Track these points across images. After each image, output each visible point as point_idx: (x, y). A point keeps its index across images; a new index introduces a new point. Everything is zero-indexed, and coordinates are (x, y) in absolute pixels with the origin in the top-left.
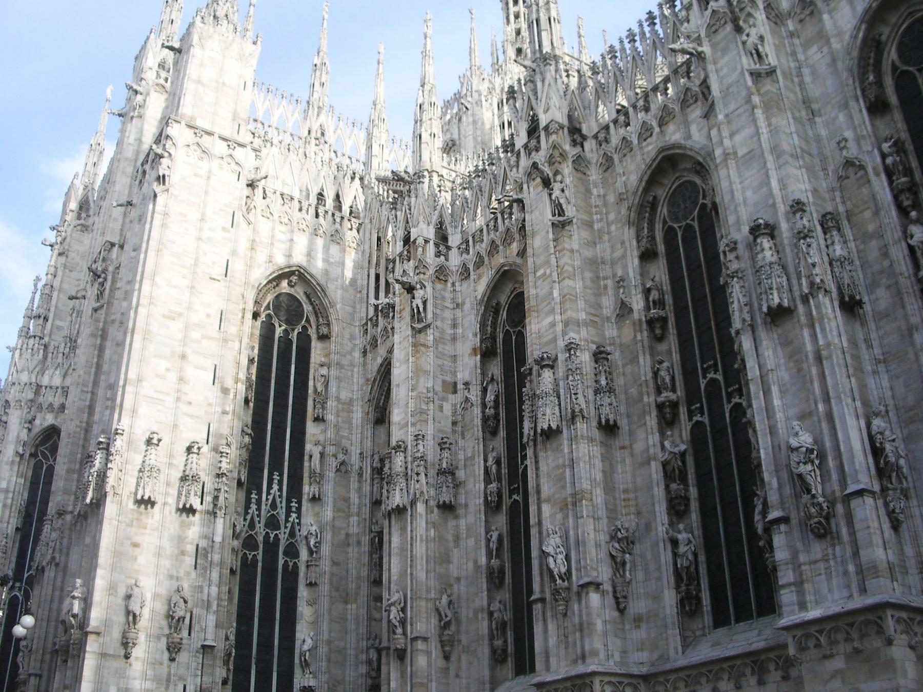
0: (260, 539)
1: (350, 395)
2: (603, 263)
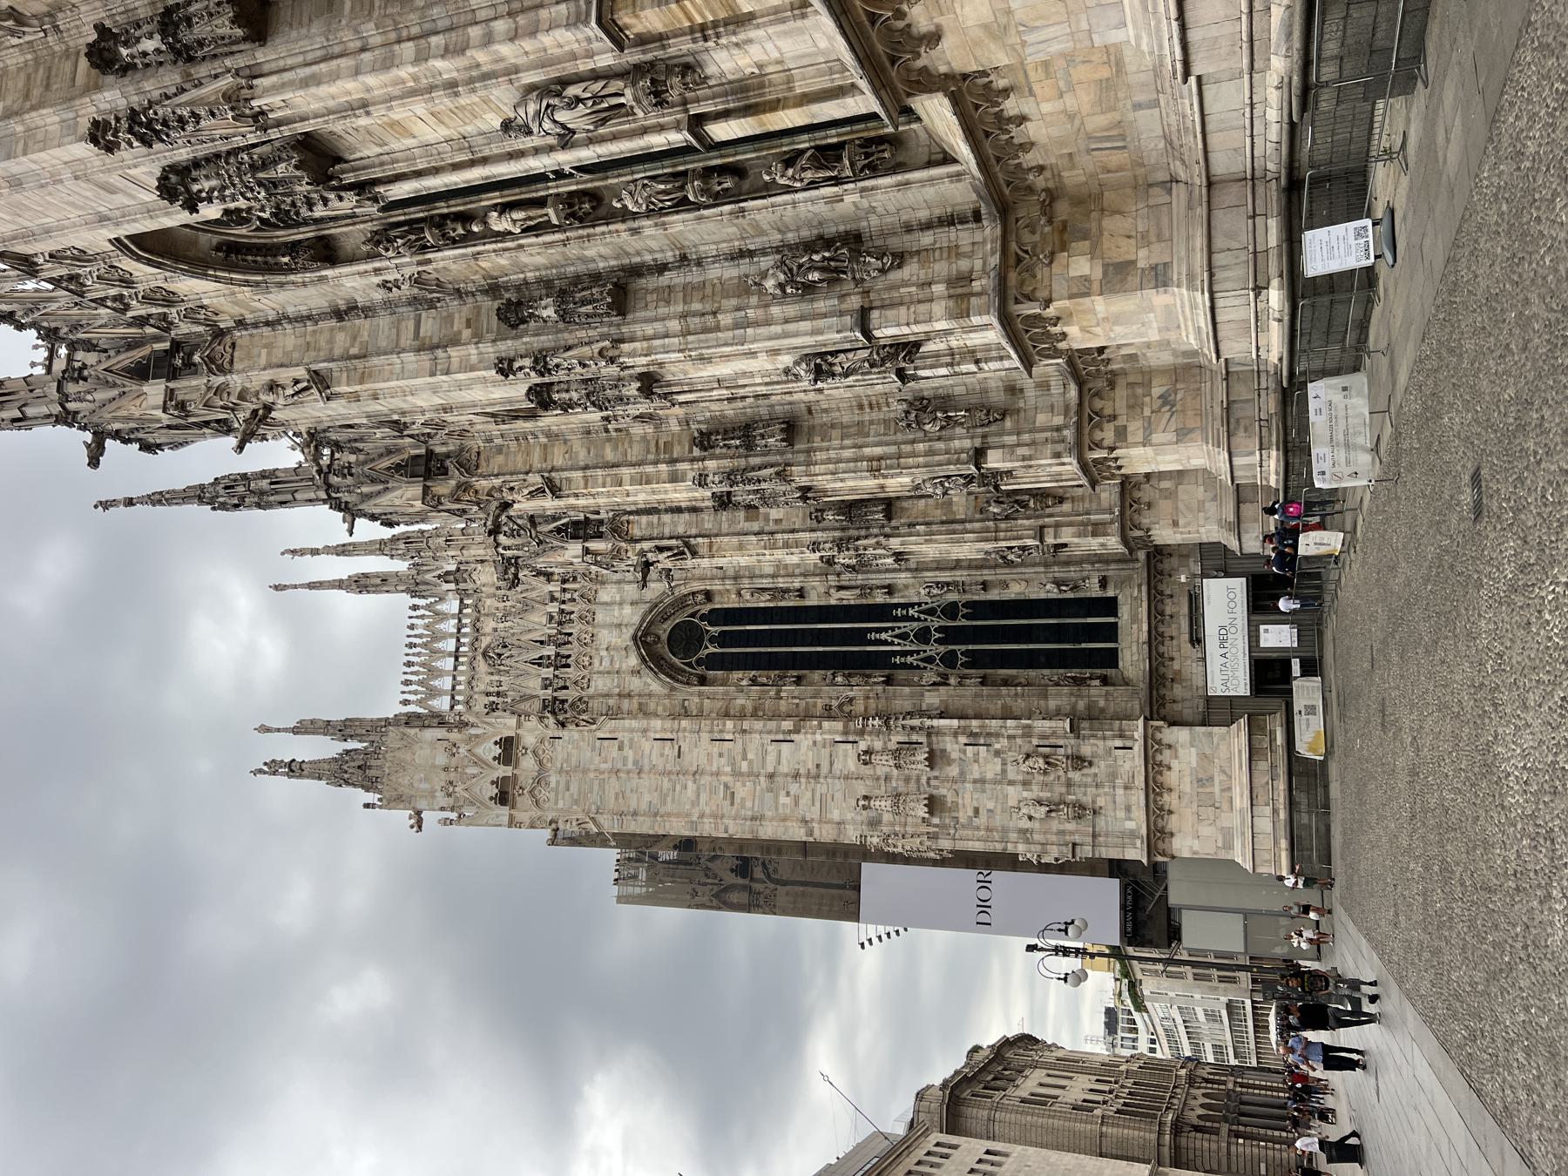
0: (942, 649)
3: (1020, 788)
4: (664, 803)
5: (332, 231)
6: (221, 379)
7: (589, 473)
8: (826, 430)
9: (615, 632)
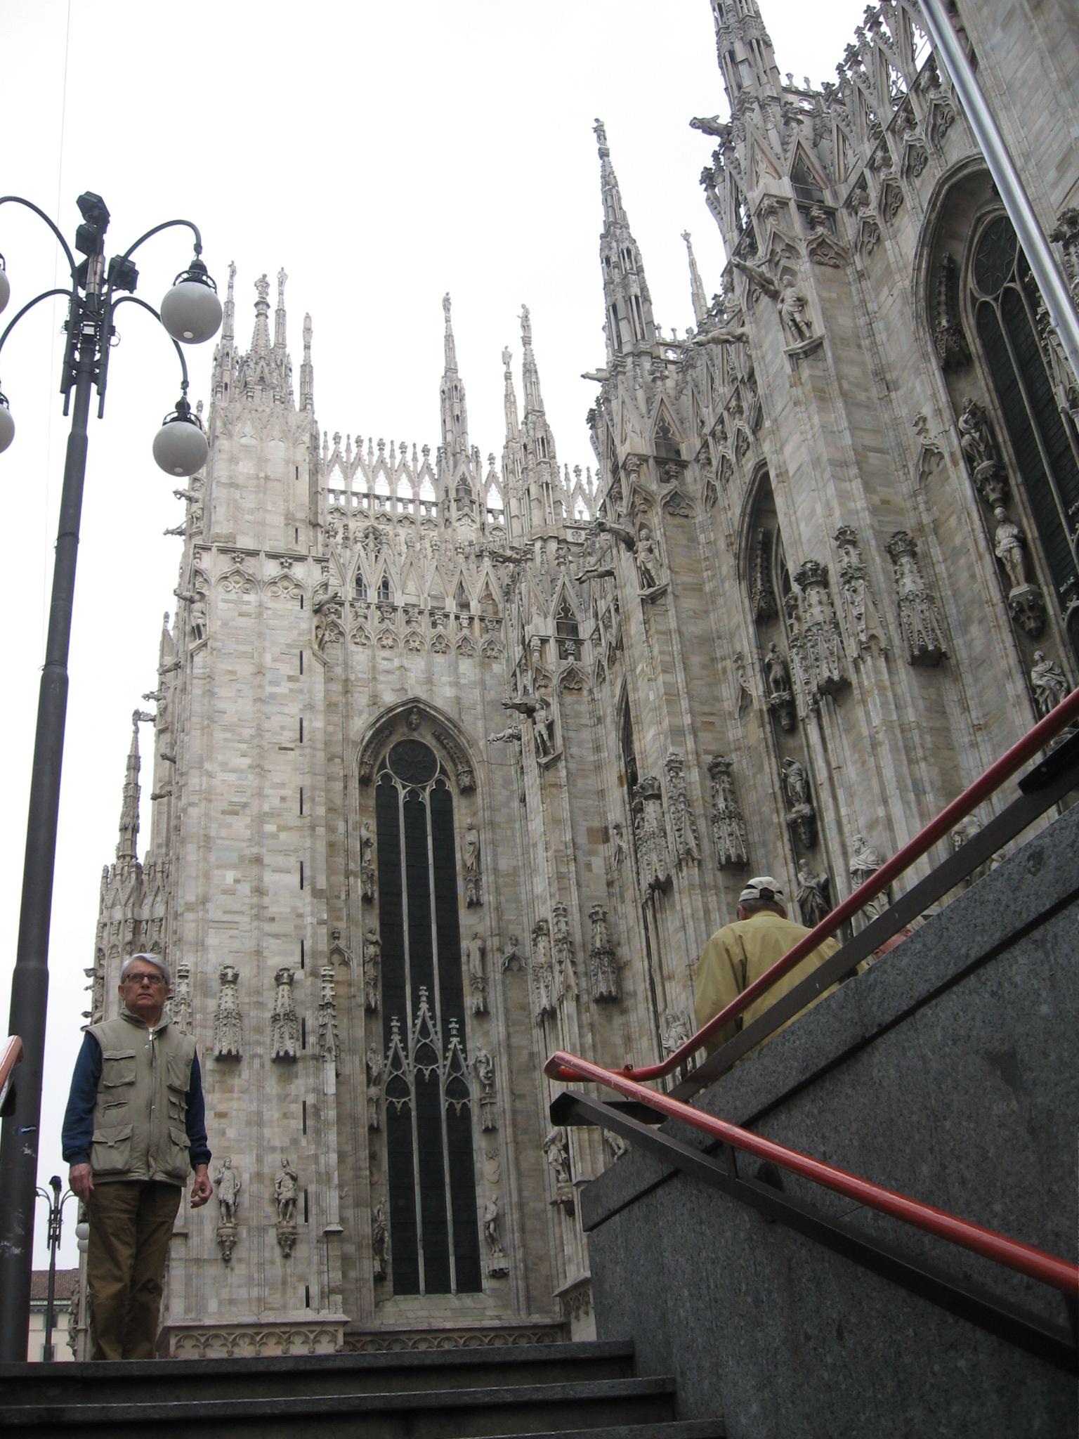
0: (410, 1079)
1: (514, 863)
2: (719, 638)
3: (254, 1169)
4: (226, 728)
5: (979, 370)
6: (803, 250)
7: (675, 636)
9: (422, 676)
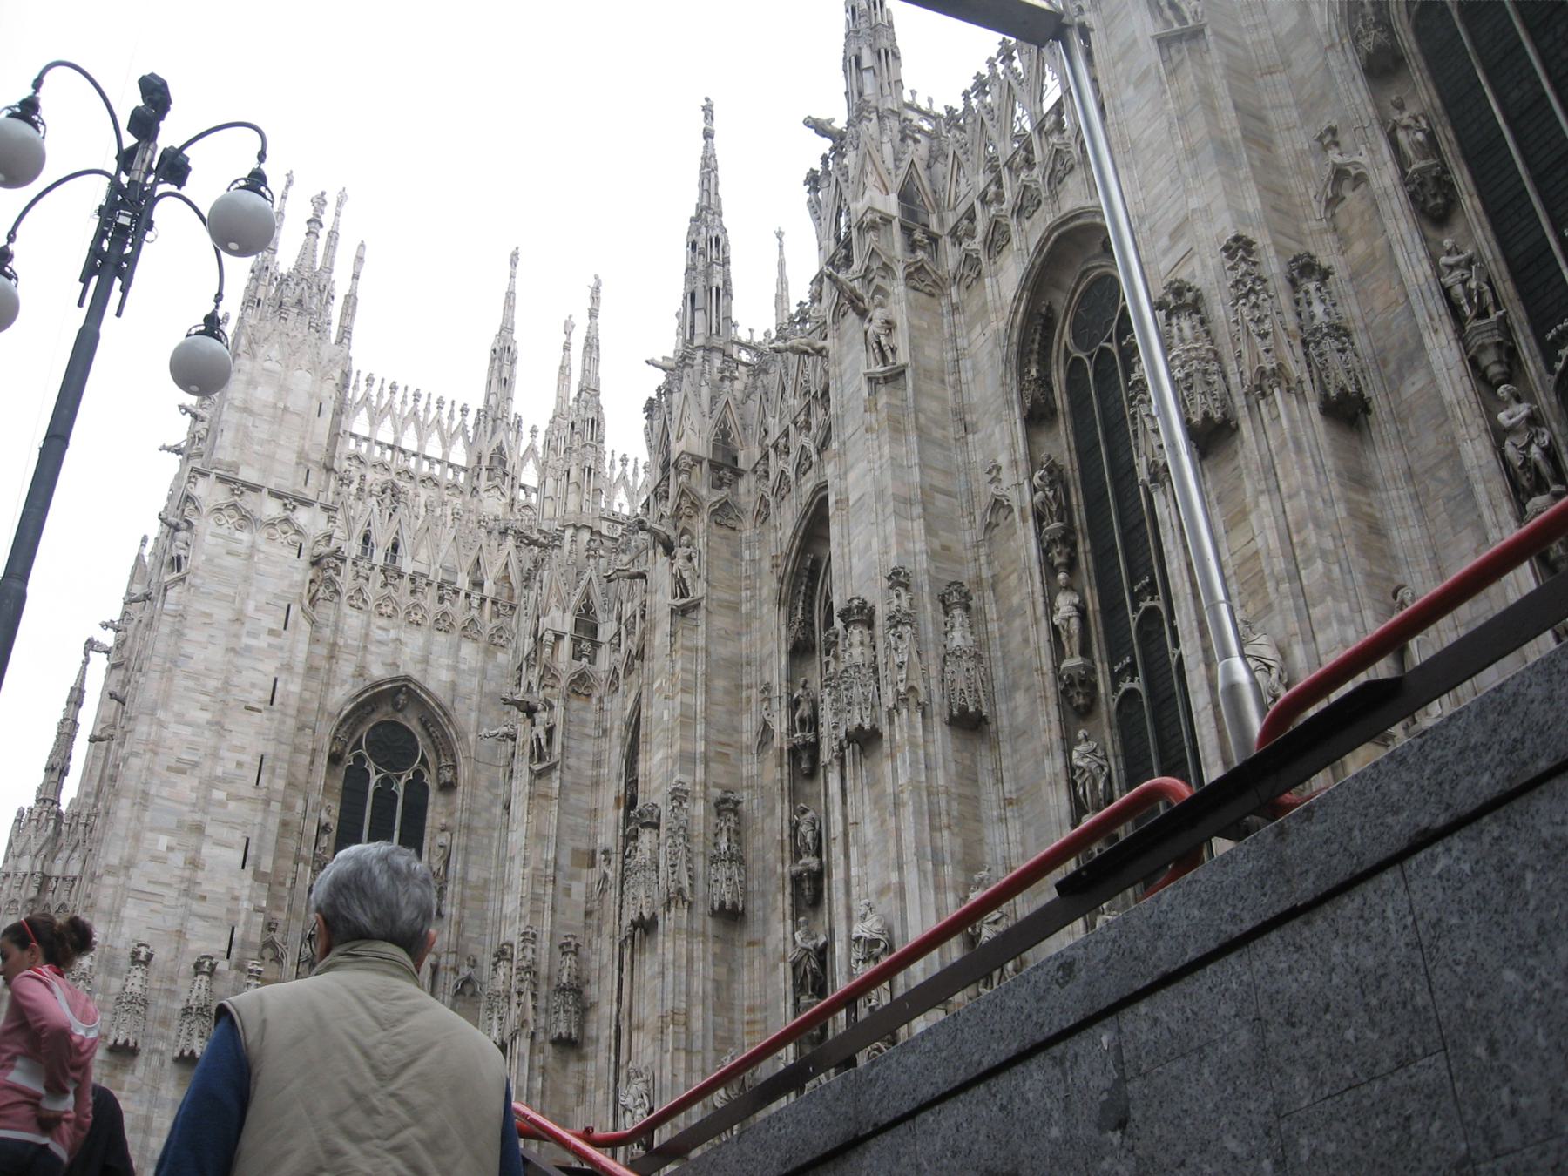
1: (485, 875)
2: (749, 664)
4: (189, 675)
5: (1062, 427)
6: (900, 272)
7: (701, 655)
8: (726, 961)
